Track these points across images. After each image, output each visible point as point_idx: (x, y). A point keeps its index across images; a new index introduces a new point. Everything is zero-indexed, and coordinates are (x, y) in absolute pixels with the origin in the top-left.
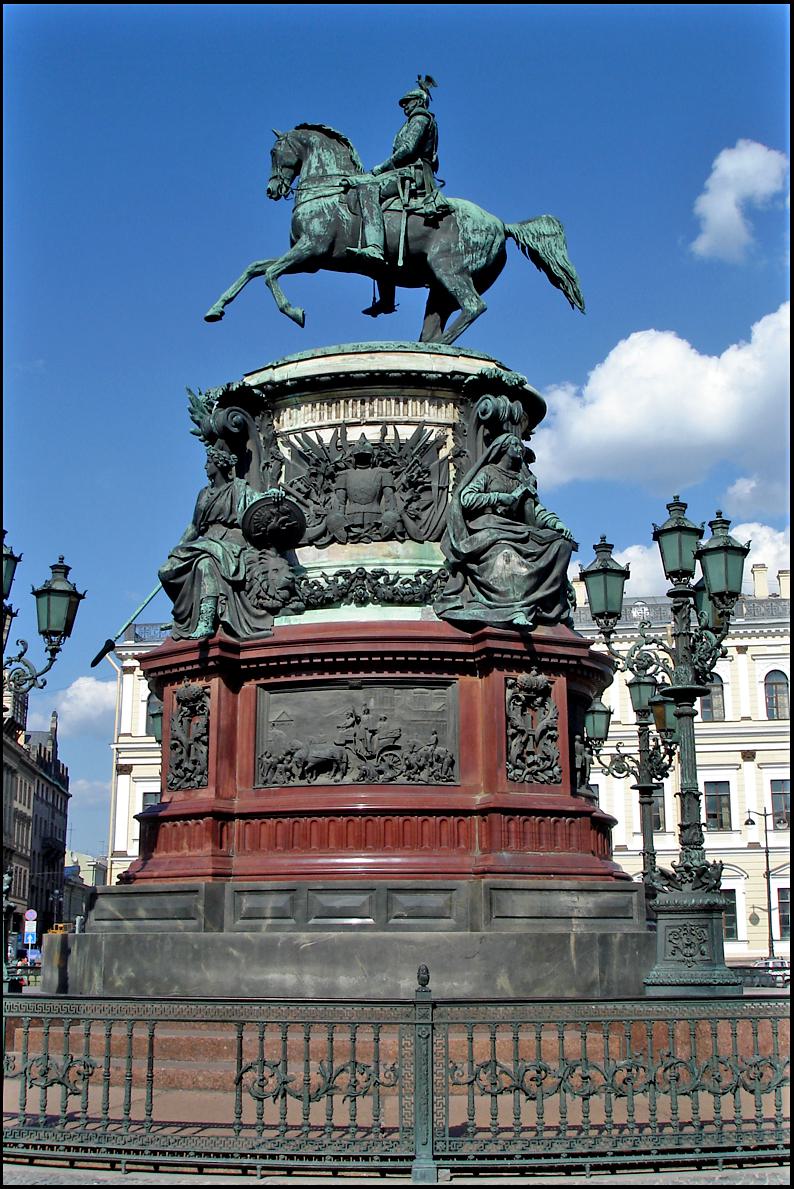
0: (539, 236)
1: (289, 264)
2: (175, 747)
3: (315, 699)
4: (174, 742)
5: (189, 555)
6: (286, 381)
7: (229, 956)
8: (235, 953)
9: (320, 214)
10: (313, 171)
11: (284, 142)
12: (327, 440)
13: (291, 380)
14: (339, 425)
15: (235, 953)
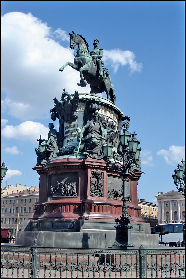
0: (113, 87)
1: (85, 69)
2: (92, 185)
3: (116, 180)
4: (92, 184)
5: (100, 139)
6: (103, 102)
7: (137, 239)
8: (138, 238)
9: (90, 61)
10: (84, 49)
11: (76, 36)
12: (105, 119)
13: (104, 103)
14: (108, 117)
15: (138, 238)
